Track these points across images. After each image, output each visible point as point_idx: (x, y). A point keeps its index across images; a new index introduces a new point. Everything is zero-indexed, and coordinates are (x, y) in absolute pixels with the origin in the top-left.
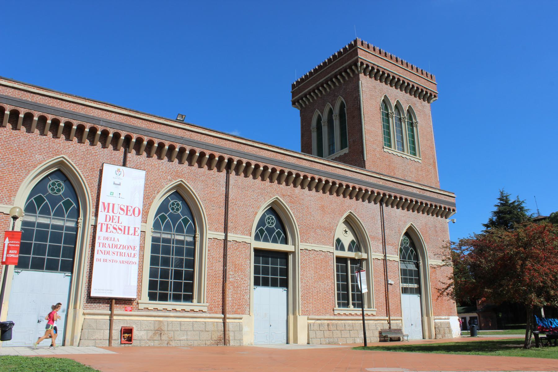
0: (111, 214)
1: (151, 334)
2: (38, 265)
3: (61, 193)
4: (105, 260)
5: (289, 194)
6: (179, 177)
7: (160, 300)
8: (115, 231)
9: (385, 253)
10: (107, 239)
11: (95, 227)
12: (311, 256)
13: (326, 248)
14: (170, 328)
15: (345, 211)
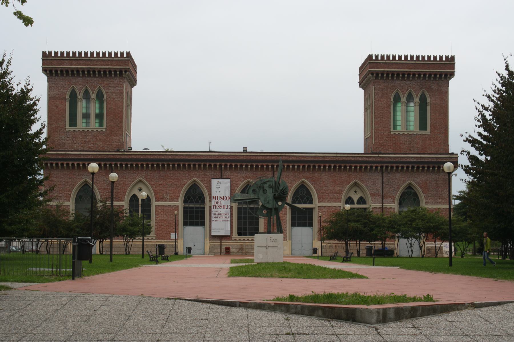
0: (217, 201)
1: (238, 250)
2: (191, 224)
3: (197, 193)
4: (216, 221)
5: (311, 176)
6: (248, 178)
7: (244, 235)
8: (219, 208)
9: (383, 203)
11: (210, 207)
12: (326, 209)
13: (335, 204)
15: (352, 180)
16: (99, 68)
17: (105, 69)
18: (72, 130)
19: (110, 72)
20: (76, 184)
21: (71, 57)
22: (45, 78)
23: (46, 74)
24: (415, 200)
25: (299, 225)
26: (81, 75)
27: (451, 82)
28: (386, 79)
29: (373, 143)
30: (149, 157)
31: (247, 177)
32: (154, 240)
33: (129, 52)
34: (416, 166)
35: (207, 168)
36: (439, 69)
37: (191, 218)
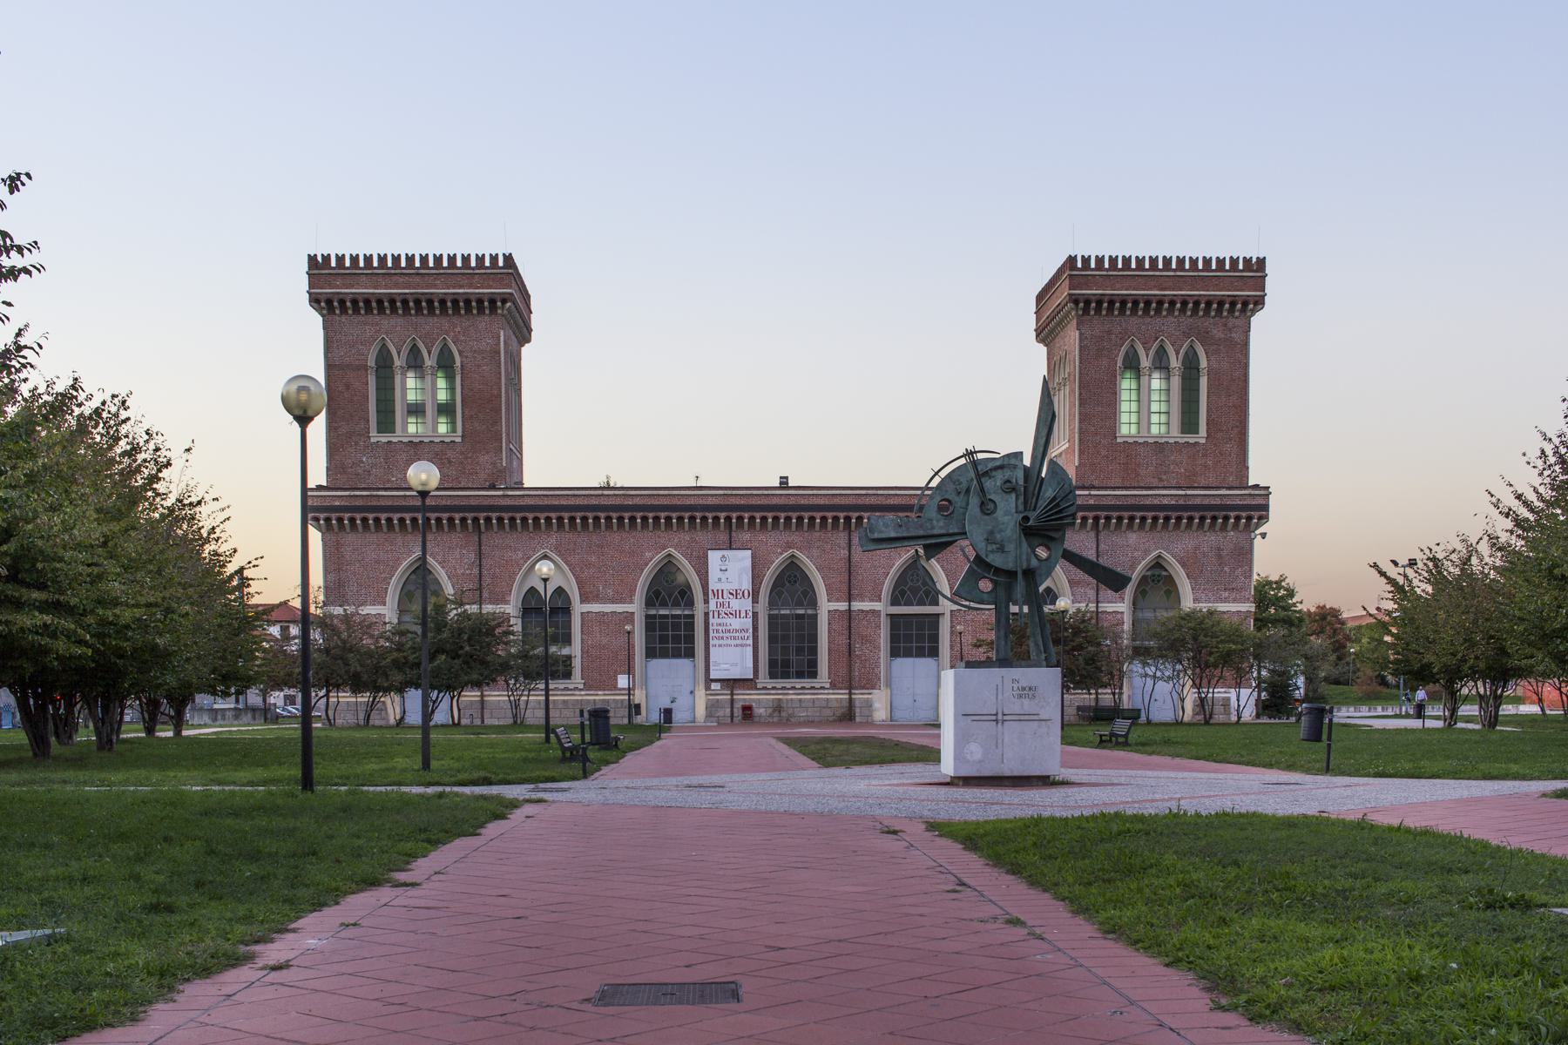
0: (721, 600)
1: (770, 711)
4: (720, 646)
6: (790, 548)
10: (720, 625)
11: (707, 614)
14: (790, 705)
16: (442, 293)
17: (455, 296)
18: (384, 440)
19: (468, 302)
20: (399, 565)
21: (375, 268)
22: (317, 320)
23: (319, 310)
24: (1168, 593)
25: (908, 654)
26: (400, 312)
27: (1258, 321)
28: (1107, 315)
29: (1077, 464)
30: (564, 502)
31: (789, 546)
32: (581, 690)
33: (510, 254)
34: (1174, 515)
35: (698, 526)
36: (1229, 290)
37: (664, 639)
